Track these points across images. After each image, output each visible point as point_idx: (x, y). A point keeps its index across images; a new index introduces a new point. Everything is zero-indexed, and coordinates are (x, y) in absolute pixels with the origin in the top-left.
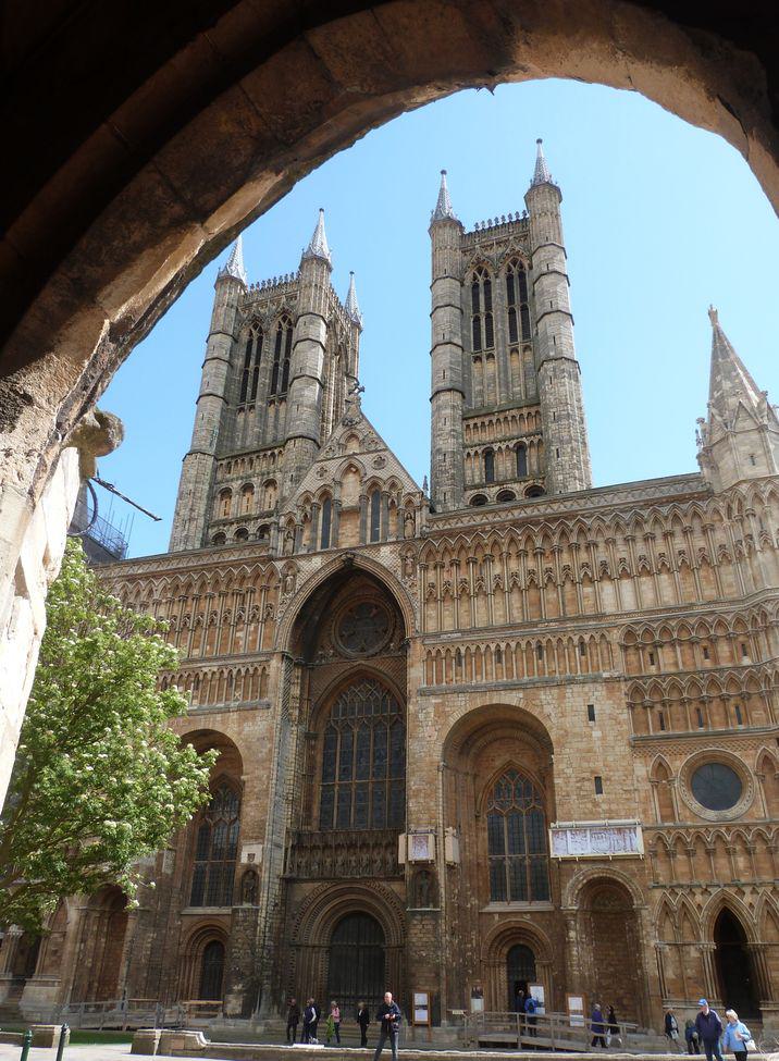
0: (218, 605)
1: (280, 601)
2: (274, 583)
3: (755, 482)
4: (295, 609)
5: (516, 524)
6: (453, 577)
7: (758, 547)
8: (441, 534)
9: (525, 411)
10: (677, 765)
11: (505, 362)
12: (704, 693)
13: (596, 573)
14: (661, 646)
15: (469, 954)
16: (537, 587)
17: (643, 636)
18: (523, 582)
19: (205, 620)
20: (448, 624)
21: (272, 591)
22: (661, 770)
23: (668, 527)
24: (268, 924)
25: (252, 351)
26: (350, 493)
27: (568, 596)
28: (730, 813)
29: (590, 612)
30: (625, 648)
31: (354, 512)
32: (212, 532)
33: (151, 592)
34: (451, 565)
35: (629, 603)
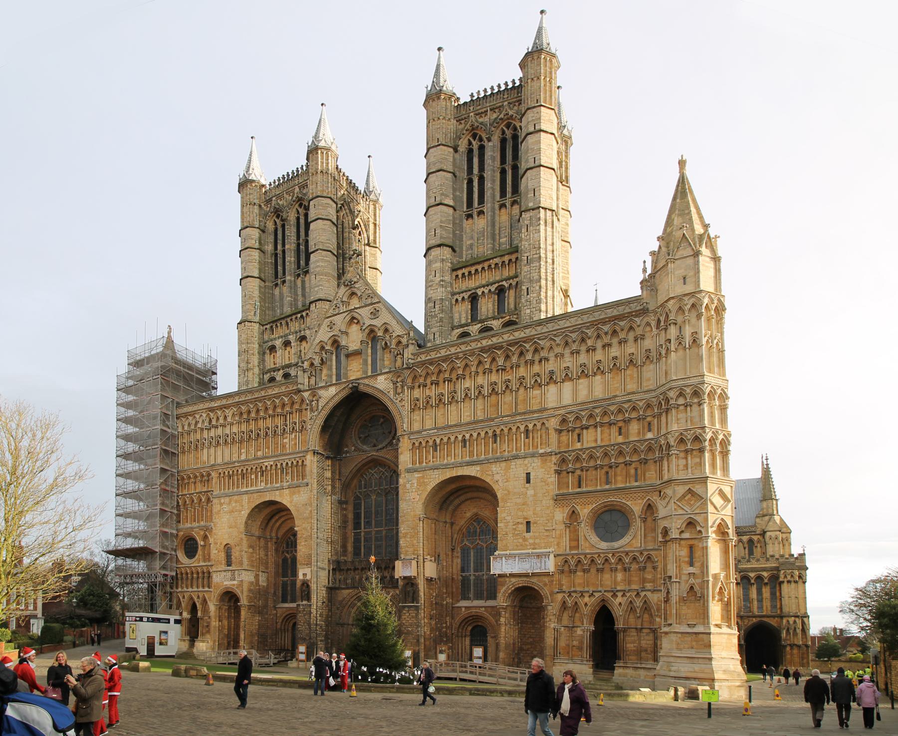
1: (309, 418)
2: (304, 406)
3: (680, 298)
4: (320, 422)
5: (483, 350)
6: (432, 392)
7: (673, 349)
9: (506, 259)
11: (493, 217)
12: (613, 461)
15: (444, 630)
16: (497, 393)
18: (485, 392)
19: (262, 433)
20: (429, 424)
21: (304, 411)
22: (573, 514)
23: (606, 340)
24: (319, 613)
33: (225, 418)
34: (432, 384)
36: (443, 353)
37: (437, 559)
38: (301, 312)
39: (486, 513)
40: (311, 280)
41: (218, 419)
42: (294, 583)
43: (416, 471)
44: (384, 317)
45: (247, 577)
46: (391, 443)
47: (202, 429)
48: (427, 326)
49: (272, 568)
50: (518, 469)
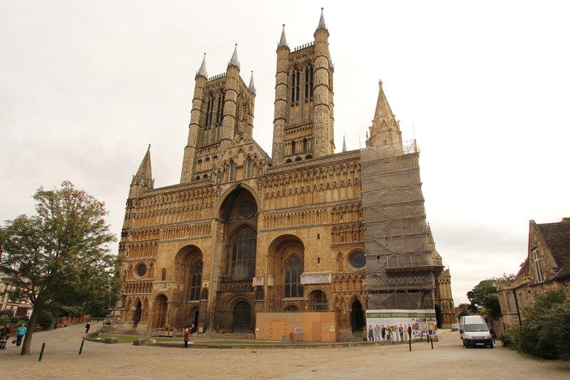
0: (195, 202)
2: (213, 194)
4: (221, 203)
6: (275, 190)
8: (271, 174)
10: (346, 253)
13: (325, 187)
14: (345, 213)
17: (339, 210)
18: (299, 191)
25: (210, 106)
26: (240, 160)
27: (315, 196)
28: (361, 269)
29: (322, 202)
30: (332, 214)
31: (241, 167)
32: (195, 176)
33: (172, 199)
35: (336, 198)
36: (280, 170)
37: (274, 277)
38: (216, 145)
39: (298, 253)
40: (223, 129)
41: (168, 199)
42: (199, 289)
43: (265, 231)
44: (255, 150)
45: (174, 286)
46: (254, 216)
47: (158, 205)
48: (273, 155)
49: (187, 281)
50: (314, 232)
